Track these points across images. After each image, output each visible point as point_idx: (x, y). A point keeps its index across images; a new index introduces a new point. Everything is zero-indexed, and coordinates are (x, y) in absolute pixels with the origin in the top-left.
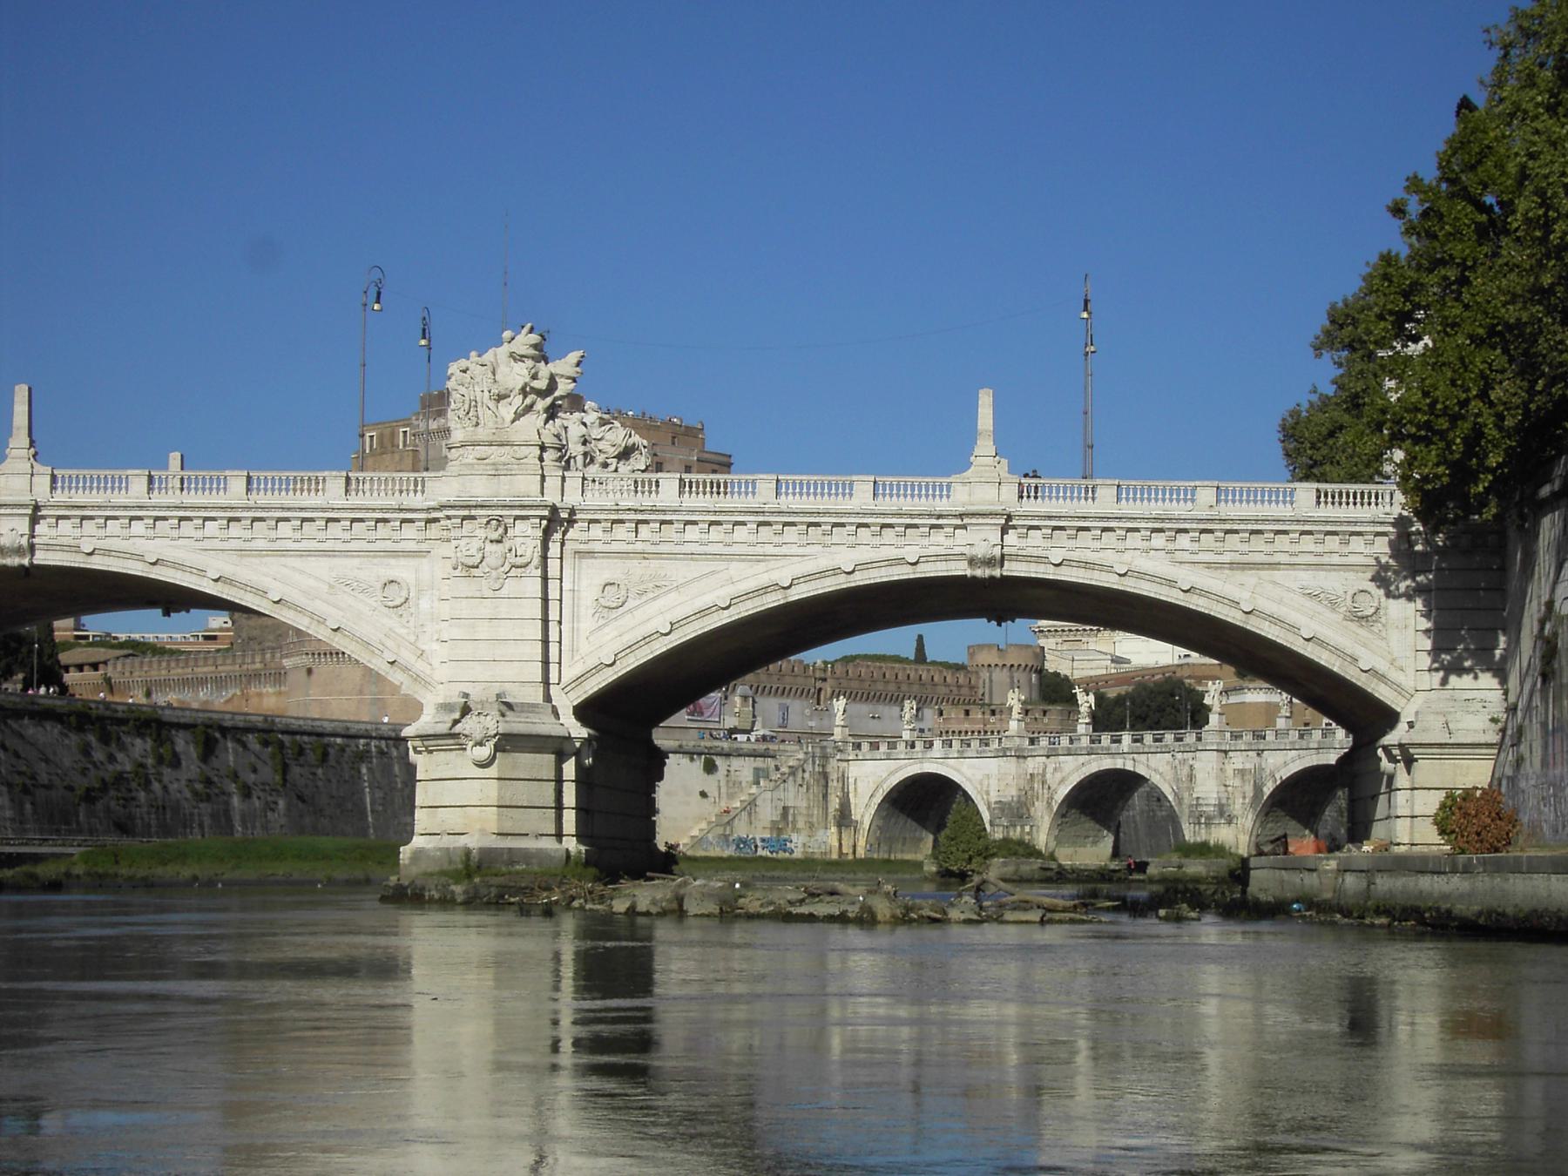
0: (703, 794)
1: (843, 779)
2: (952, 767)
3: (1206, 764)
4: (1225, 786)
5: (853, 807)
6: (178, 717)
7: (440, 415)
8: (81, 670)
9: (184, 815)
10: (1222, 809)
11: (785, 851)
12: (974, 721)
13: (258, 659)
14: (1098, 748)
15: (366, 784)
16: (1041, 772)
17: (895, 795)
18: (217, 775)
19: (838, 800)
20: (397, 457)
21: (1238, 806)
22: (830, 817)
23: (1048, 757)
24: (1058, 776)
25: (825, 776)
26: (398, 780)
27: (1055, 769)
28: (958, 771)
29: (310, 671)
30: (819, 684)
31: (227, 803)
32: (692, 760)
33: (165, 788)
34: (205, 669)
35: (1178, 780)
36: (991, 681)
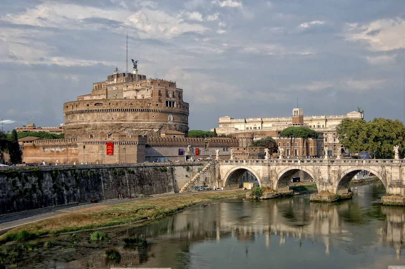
0: (187, 176)
1: (219, 169)
2: (249, 167)
3: (324, 170)
4: (330, 175)
5: (221, 176)
6: (46, 169)
8: (28, 143)
9: (49, 199)
10: (330, 182)
12: (240, 151)
14: (291, 164)
15: (102, 182)
16: (274, 169)
17: (232, 174)
20: (102, 90)
21: (333, 180)
24: (279, 170)
25: (215, 169)
26: (111, 180)
27: (278, 169)
28: (251, 168)
29: (84, 147)
30: (206, 144)
31: (62, 193)
32: (184, 167)
33: (42, 191)
34: (57, 143)
35: (314, 172)
36: (242, 141)
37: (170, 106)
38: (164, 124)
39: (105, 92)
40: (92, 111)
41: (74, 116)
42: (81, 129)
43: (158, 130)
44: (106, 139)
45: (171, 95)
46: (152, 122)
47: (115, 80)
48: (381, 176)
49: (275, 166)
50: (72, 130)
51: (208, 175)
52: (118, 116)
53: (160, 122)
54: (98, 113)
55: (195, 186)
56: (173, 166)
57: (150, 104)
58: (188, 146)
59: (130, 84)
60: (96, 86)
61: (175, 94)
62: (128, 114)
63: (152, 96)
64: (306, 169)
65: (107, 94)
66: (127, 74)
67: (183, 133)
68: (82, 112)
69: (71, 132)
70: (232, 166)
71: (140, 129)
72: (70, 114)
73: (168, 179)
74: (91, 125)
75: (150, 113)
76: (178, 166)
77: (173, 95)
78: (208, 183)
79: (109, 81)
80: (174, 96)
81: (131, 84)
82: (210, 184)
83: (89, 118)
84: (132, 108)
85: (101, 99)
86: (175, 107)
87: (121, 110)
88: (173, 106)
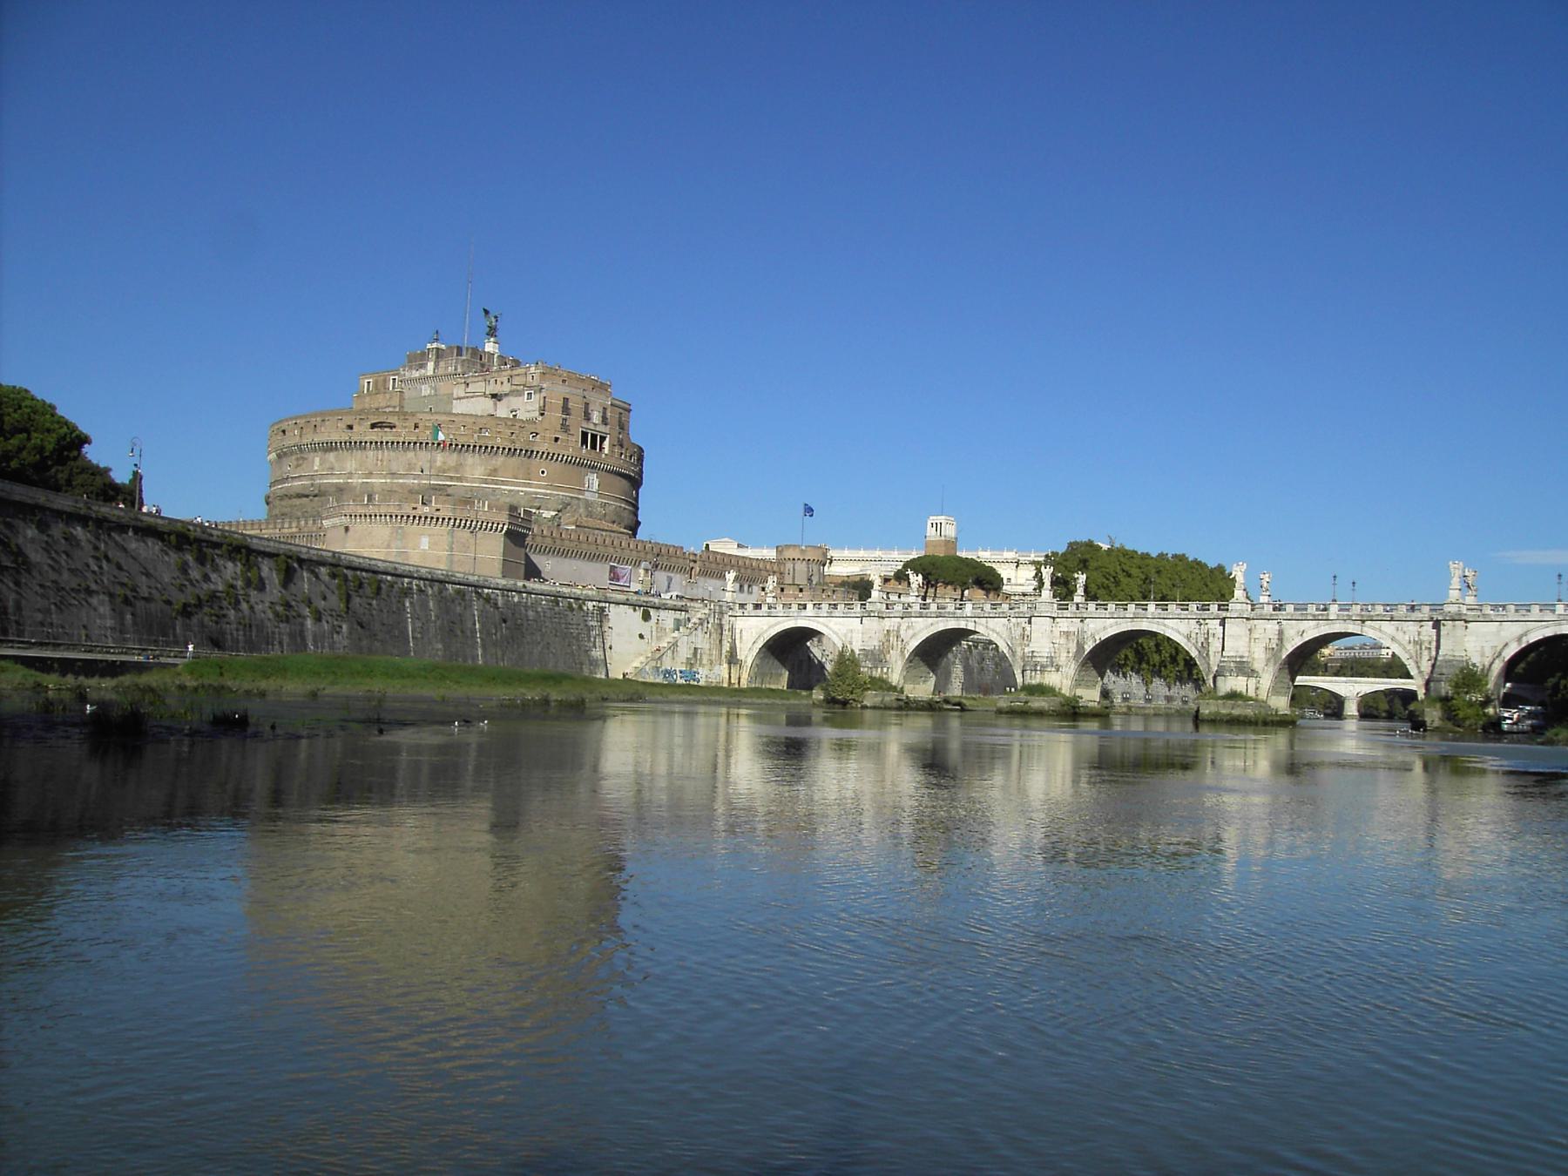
0: (641, 636)
1: (732, 629)
7: (421, 368)
11: (694, 680)
13: (294, 525)
14: (945, 612)
15: (409, 615)
16: (896, 628)
17: (770, 643)
18: (294, 600)
19: (728, 645)
20: (388, 396)
22: (723, 656)
23: (902, 618)
24: (911, 632)
25: (721, 626)
27: (908, 627)
29: (347, 529)
30: (692, 564)
31: (302, 625)
32: (635, 610)
33: (252, 608)
36: (794, 569)
37: (594, 447)
38: (572, 497)
40: (361, 446)
42: (323, 498)
43: (554, 513)
44: (414, 508)
45: (596, 417)
46: (537, 489)
47: (431, 365)
48: (1196, 648)
49: (899, 619)
50: (297, 502)
51: (702, 641)
52: (438, 464)
53: (561, 491)
55: (663, 668)
56: (606, 602)
57: (537, 434)
58: (643, 564)
59: (476, 379)
60: (369, 383)
61: (609, 414)
62: (470, 459)
63: (542, 414)
64: (987, 627)
66: (467, 349)
67: (625, 531)
68: (330, 447)
69: (291, 506)
72: (292, 453)
73: (589, 640)
74: (356, 487)
77: (603, 417)
78: (703, 666)
79: (411, 368)
80: (604, 421)
81: (480, 378)
82: (707, 668)
83: (351, 466)
84: (481, 442)
86: (606, 451)
87: (451, 445)
88: (601, 448)
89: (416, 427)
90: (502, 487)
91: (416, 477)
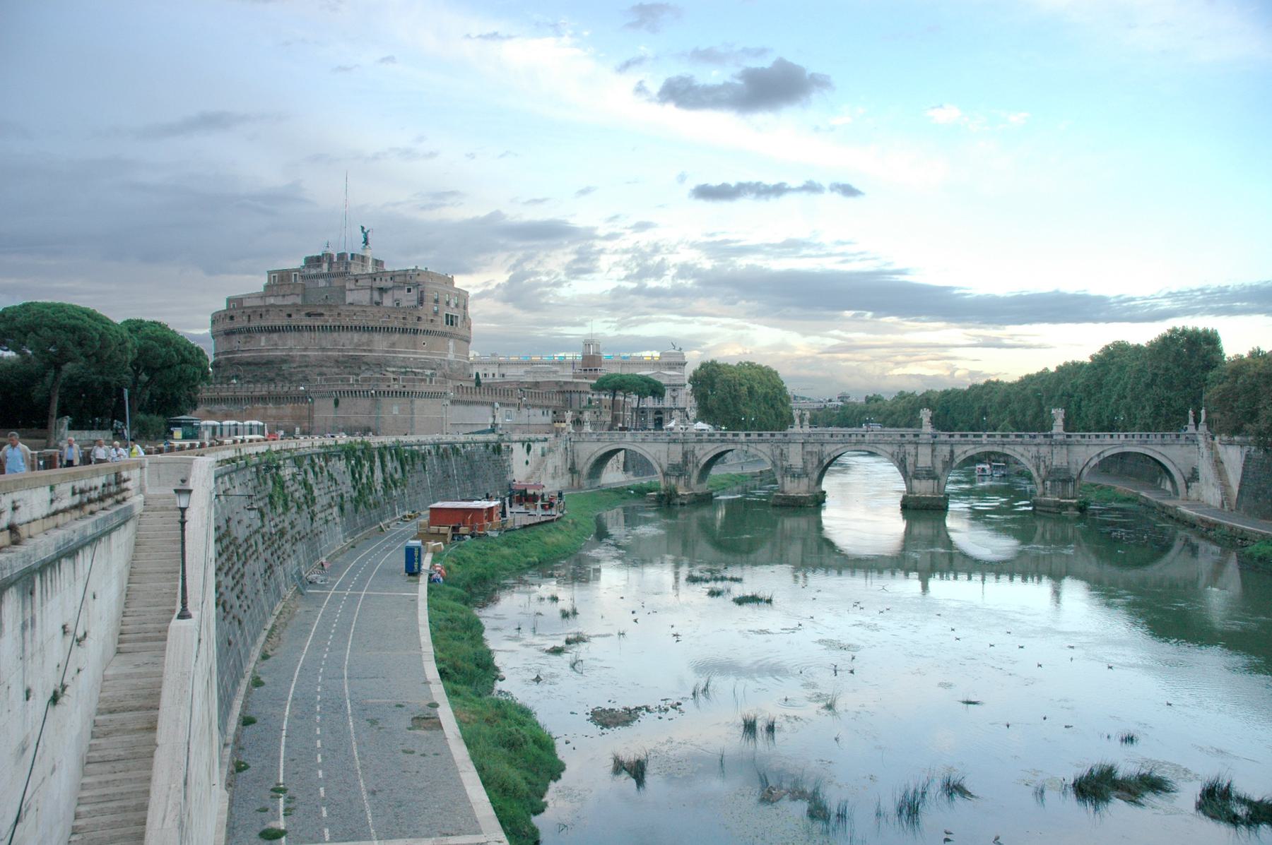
20: (292, 287)
21: (809, 468)
24: (702, 452)
27: (700, 449)
32: (523, 445)
35: (773, 455)
37: (452, 324)
39: (299, 290)
40: (298, 329)
41: (251, 337)
45: (452, 305)
46: (421, 354)
47: (325, 266)
54: (313, 333)
60: (274, 277)
62: (377, 337)
65: (304, 296)
70: (601, 445)
71: (401, 368)
75: (419, 336)
76: (516, 442)
79: (309, 267)
80: (457, 306)
85: (289, 303)
88: (456, 324)
89: (339, 314)
90: (400, 355)
91: (339, 350)
